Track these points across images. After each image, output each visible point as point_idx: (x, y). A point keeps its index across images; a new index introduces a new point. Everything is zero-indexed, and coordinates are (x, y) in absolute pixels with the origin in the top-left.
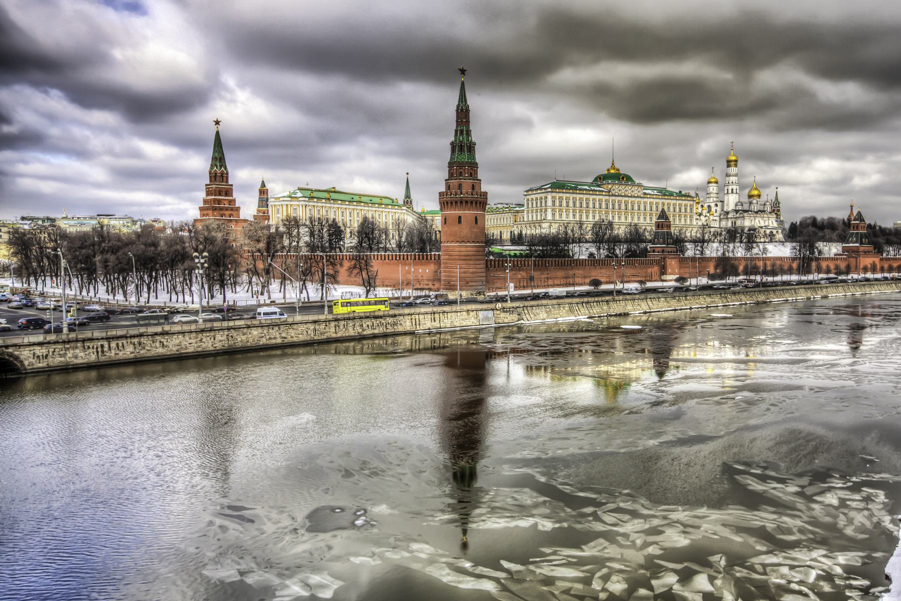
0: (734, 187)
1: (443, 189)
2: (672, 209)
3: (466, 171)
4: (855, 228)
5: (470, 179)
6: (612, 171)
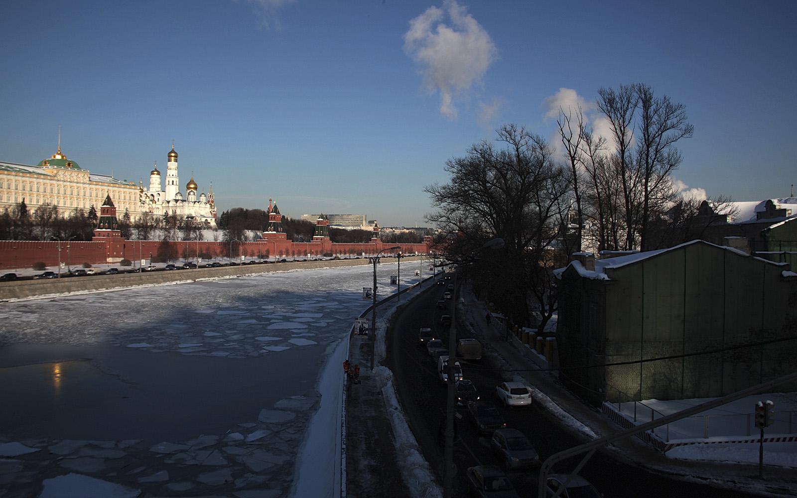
0: (175, 180)
2: (117, 197)
4: (273, 218)
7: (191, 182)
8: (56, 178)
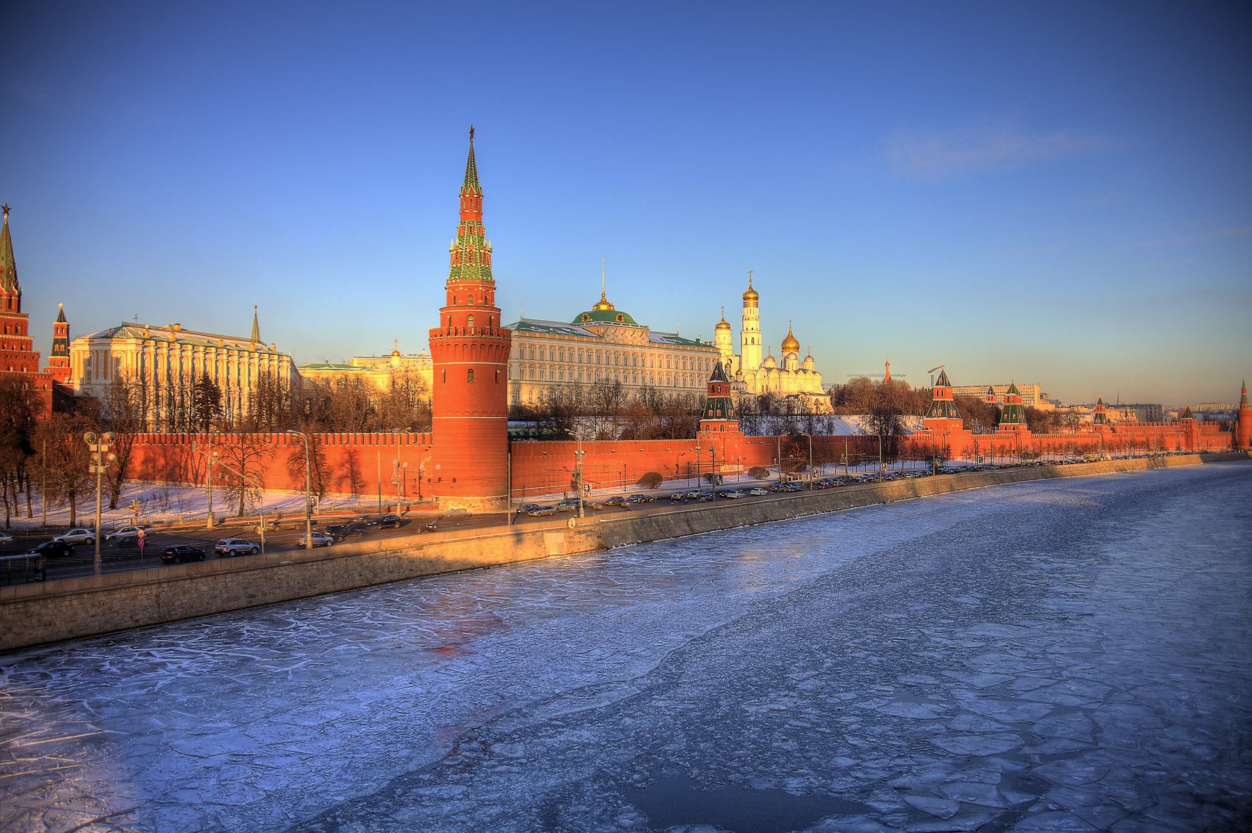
0: (756, 336)
1: (437, 324)
3: (479, 294)
6: (604, 307)
7: (790, 338)
8: (604, 341)
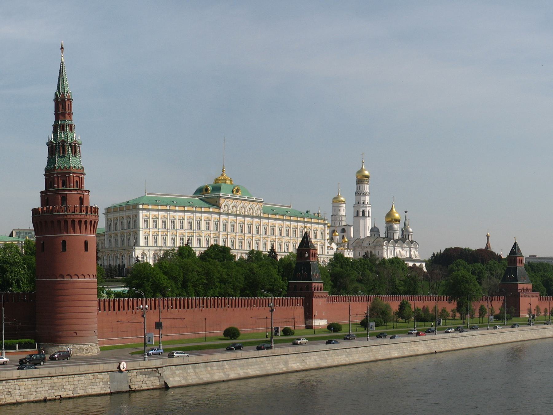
5: (76, 190)
